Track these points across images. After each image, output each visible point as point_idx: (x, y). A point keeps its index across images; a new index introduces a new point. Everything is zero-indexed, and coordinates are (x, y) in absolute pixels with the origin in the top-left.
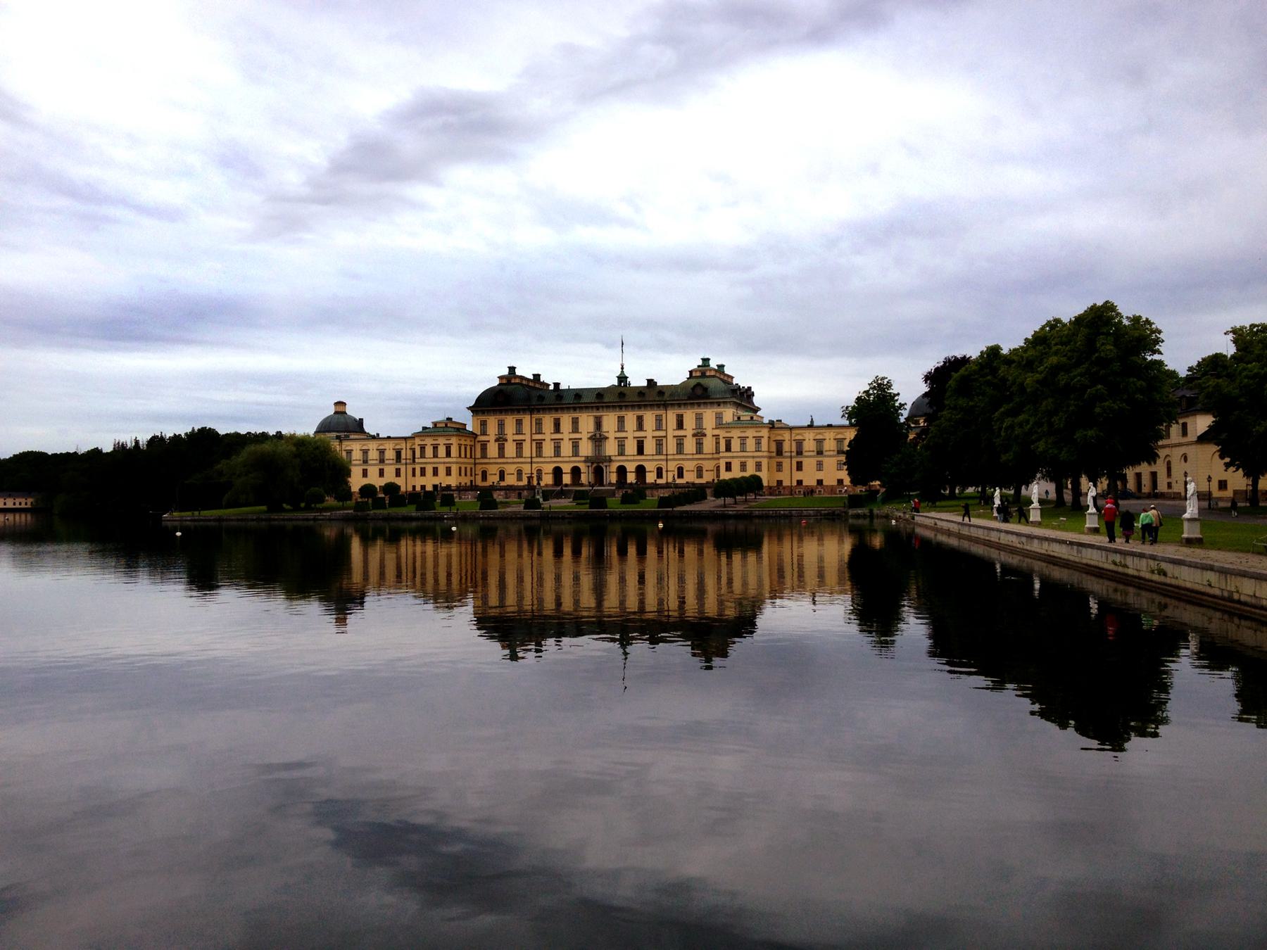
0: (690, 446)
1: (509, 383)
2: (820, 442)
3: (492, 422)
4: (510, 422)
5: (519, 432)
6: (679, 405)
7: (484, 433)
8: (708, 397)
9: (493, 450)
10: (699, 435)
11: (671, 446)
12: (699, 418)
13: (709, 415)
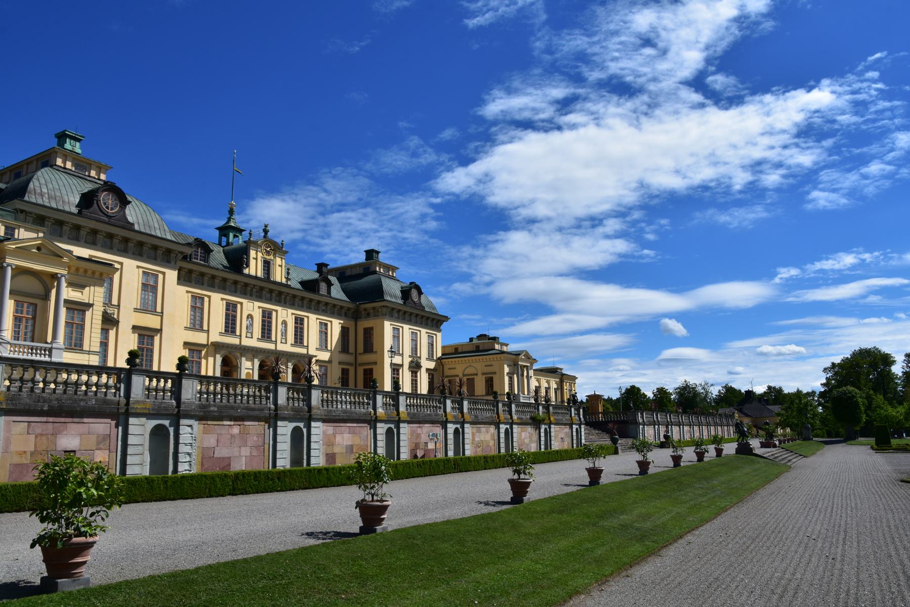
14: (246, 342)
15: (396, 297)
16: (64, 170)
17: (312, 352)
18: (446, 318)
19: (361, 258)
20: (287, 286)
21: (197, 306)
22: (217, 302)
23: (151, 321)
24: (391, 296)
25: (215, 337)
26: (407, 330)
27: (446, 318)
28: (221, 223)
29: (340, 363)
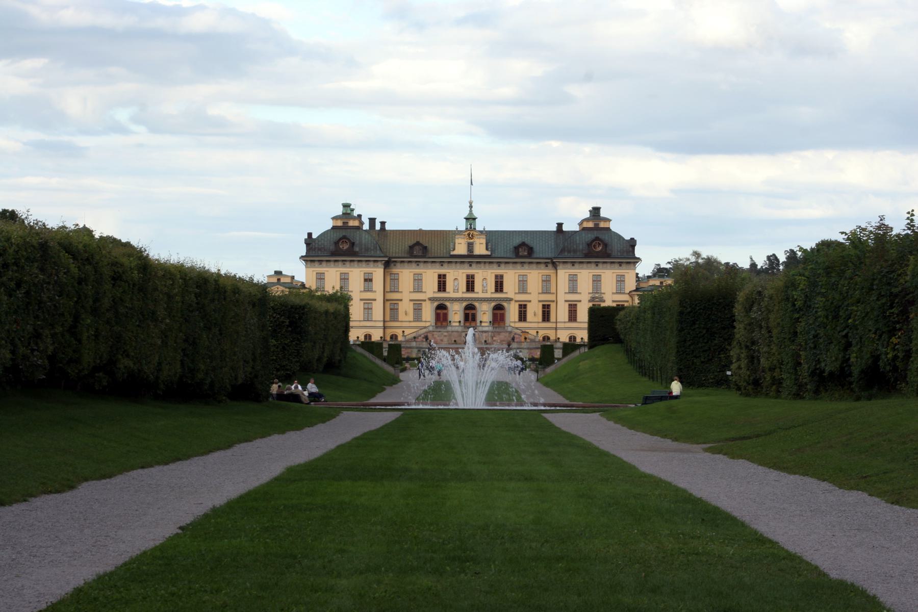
1: (345, 227)
5: (368, 289)
6: (573, 264)
12: (597, 280)
13: (609, 276)
15: (575, 251)
17: (510, 295)
21: (418, 280)
22: (430, 276)
23: (368, 295)
24: (569, 252)
25: (431, 295)
26: (585, 275)
27: (639, 259)
28: (466, 214)
29: (540, 301)
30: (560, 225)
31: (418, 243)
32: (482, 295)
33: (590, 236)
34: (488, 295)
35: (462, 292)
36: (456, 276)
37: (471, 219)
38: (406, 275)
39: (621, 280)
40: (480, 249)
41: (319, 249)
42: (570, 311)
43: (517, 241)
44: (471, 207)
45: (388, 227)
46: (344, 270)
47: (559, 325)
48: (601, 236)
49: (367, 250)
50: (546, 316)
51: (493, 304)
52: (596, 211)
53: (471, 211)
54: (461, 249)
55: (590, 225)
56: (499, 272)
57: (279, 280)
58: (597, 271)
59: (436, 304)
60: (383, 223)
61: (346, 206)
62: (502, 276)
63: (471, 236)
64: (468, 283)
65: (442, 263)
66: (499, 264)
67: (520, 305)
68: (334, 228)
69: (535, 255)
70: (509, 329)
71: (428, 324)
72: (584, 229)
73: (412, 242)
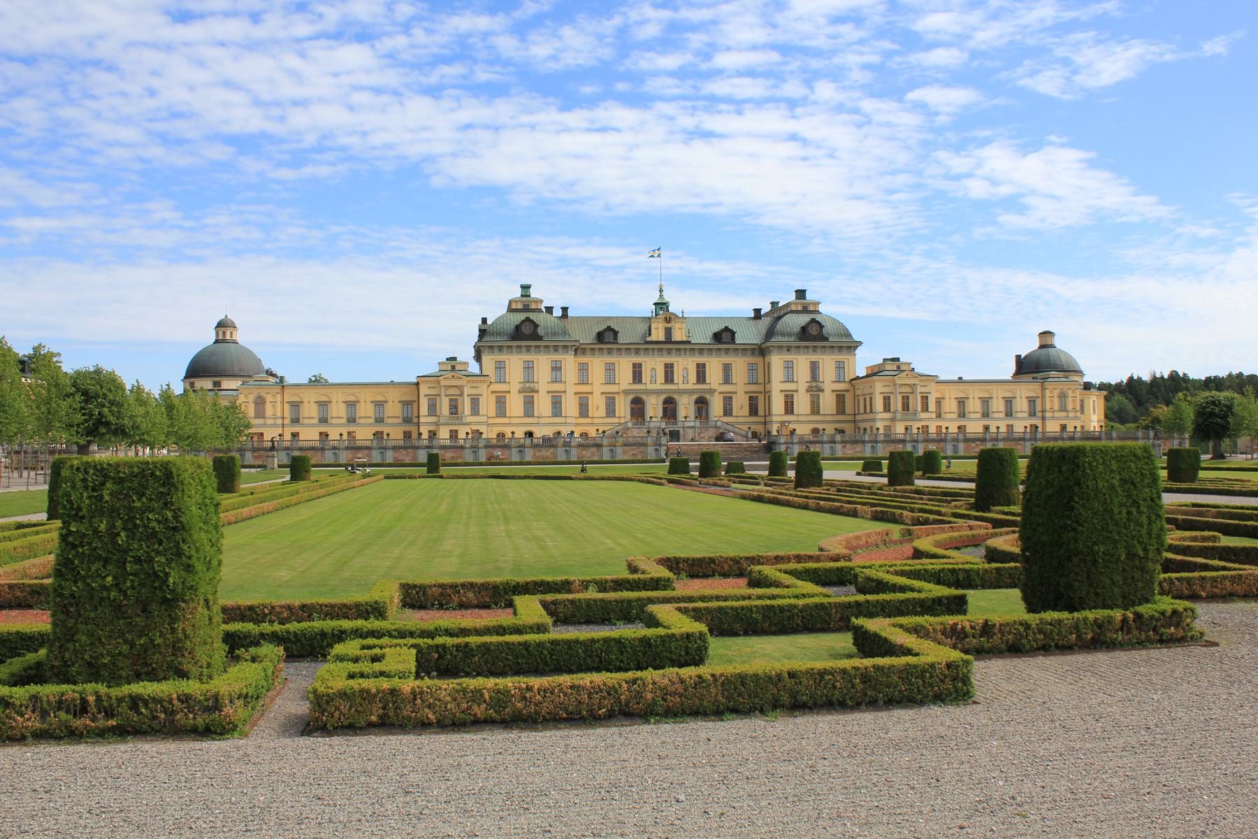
0: (802, 403)
1: (526, 309)
2: (985, 402)
3: (515, 362)
4: (543, 362)
6: (789, 349)
7: (501, 380)
8: (826, 339)
9: (515, 405)
10: (815, 390)
11: (778, 405)
12: (814, 367)
13: (827, 363)
14: (650, 387)
15: (789, 335)
16: (517, 310)
17: (713, 386)
18: (860, 343)
19: (792, 297)
20: (689, 342)
21: (610, 369)
22: (624, 365)
24: (783, 335)
25: (626, 387)
26: (802, 362)
27: (860, 343)
30: (757, 311)
31: (609, 329)
32: (682, 387)
33: (804, 319)
34: (690, 386)
35: (659, 384)
36: (653, 365)
37: (661, 306)
38: (597, 364)
39: (840, 367)
40: (678, 336)
41: (499, 334)
42: (786, 403)
43: (717, 327)
44: (661, 291)
45: (570, 313)
46: (528, 357)
47: (774, 419)
48: (818, 318)
49: (554, 334)
50: (753, 410)
51: (695, 397)
52: (801, 294)
53: (661, 296)
54: (658, 334)
55: (800, 308)
56: (701, 360)
57: (453, 367)
58: (814, 358)
59: (631, 397)
60: (565, 309)
61: (525, 288)
62: (704, 365)
63: (668, 320)
64: (666, 373)
65: (637, 351)
66: (701, 351)
67: (725, 399)
68: (510, 310)
69: (738, 341)
70: (719, 424)
71: (622, 421)
72: (792, 312)
73: (602, 327)
